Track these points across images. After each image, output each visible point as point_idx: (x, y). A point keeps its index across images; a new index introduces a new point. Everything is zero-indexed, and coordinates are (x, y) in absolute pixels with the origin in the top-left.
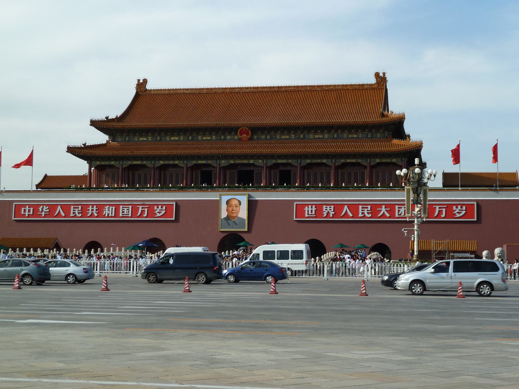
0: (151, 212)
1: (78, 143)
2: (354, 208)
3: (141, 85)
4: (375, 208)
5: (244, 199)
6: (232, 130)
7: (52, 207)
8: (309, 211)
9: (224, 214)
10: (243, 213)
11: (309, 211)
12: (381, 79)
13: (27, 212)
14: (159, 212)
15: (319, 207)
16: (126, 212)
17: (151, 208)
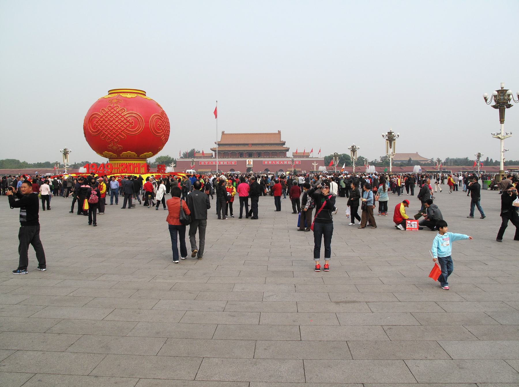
0: (231, 163)
1: (212, 147)
2: (275, 162)
3: (223, 133)
4: (280, 162)
5: (252, 160)
6: (247, 144)
7: (209, 162)
8: (266, 163)
9: (247, 163)
10: (252, 163)
11: (266, 163)
12: (279, 132)
13: (203, 163)
14: (233, 163)
15: (268, 162)
16: (225, 163)
17: (231, 162)
